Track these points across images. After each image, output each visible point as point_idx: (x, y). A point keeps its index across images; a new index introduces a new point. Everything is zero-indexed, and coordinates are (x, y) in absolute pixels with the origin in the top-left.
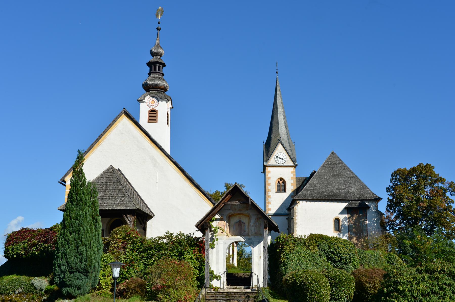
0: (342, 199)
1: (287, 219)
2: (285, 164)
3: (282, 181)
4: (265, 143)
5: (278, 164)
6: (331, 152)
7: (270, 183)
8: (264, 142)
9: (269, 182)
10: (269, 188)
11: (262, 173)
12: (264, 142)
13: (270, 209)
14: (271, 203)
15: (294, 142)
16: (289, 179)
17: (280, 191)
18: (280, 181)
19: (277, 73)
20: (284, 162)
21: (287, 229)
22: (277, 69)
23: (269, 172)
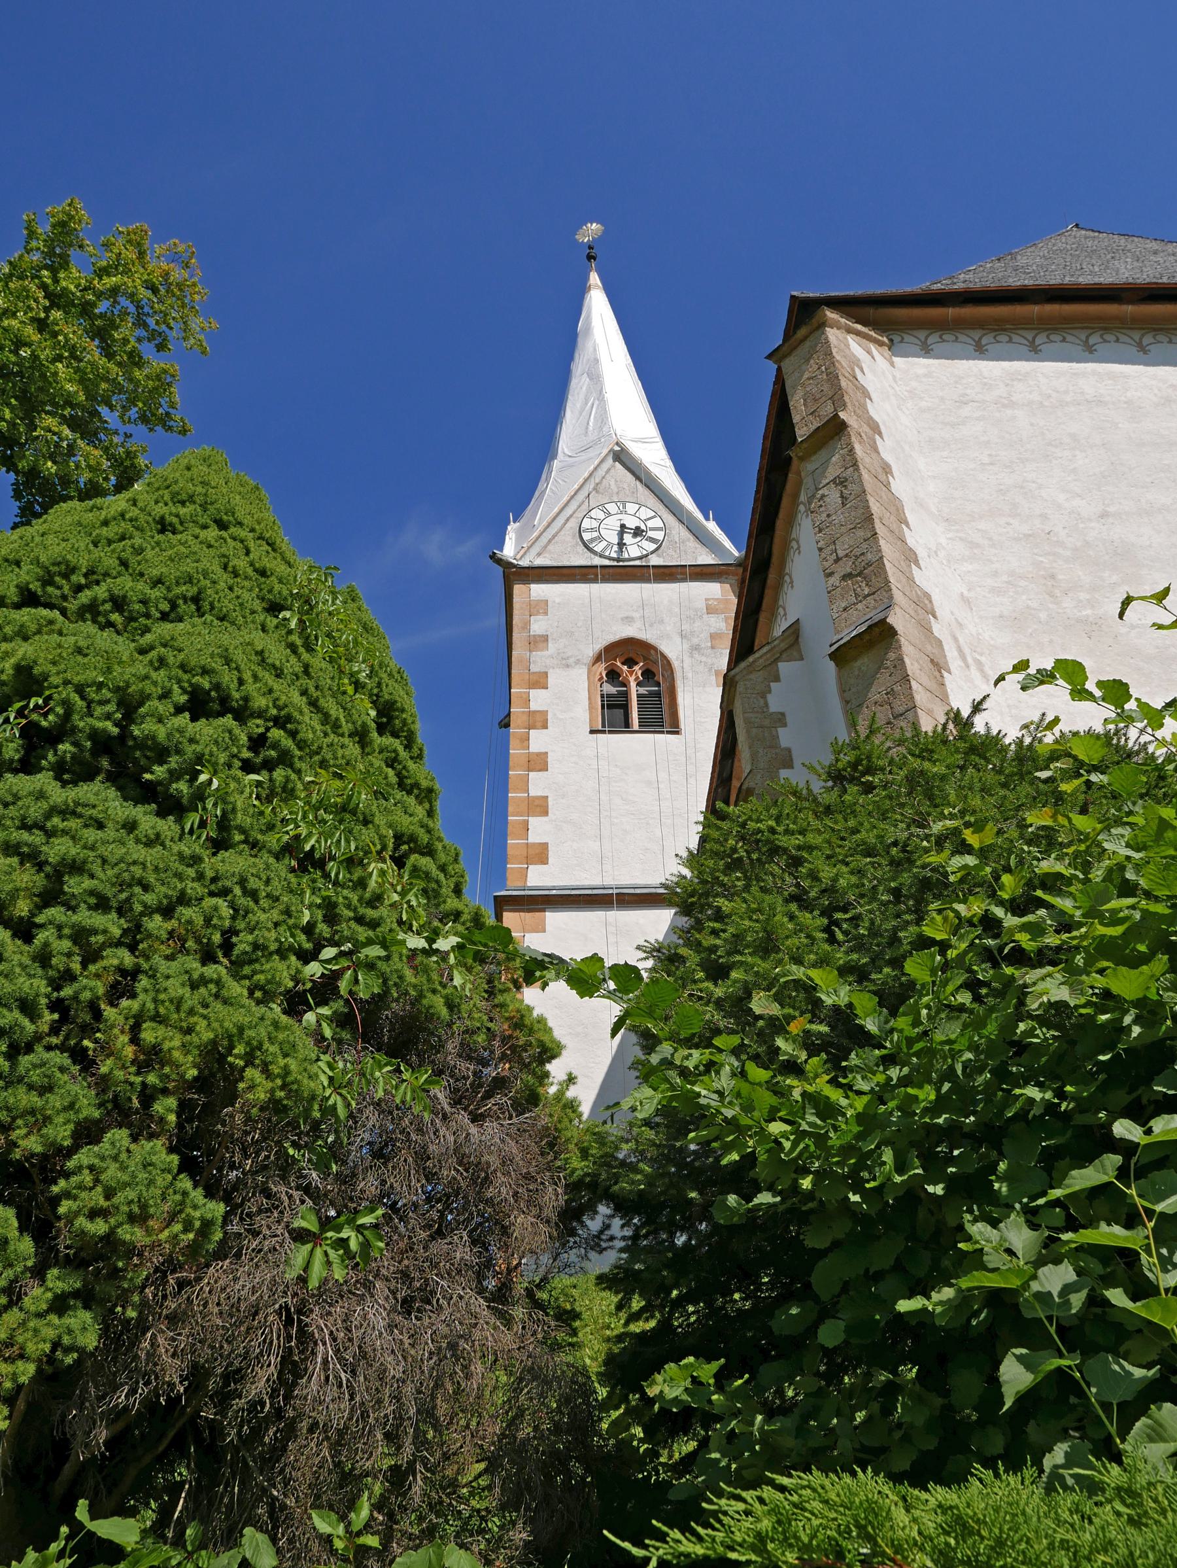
2: (655, 560)
5: (607, 562)
9: (534, 668)
13: (540, 855)
16: (696, 648)
17: (627, 723)
23: (541, 607)
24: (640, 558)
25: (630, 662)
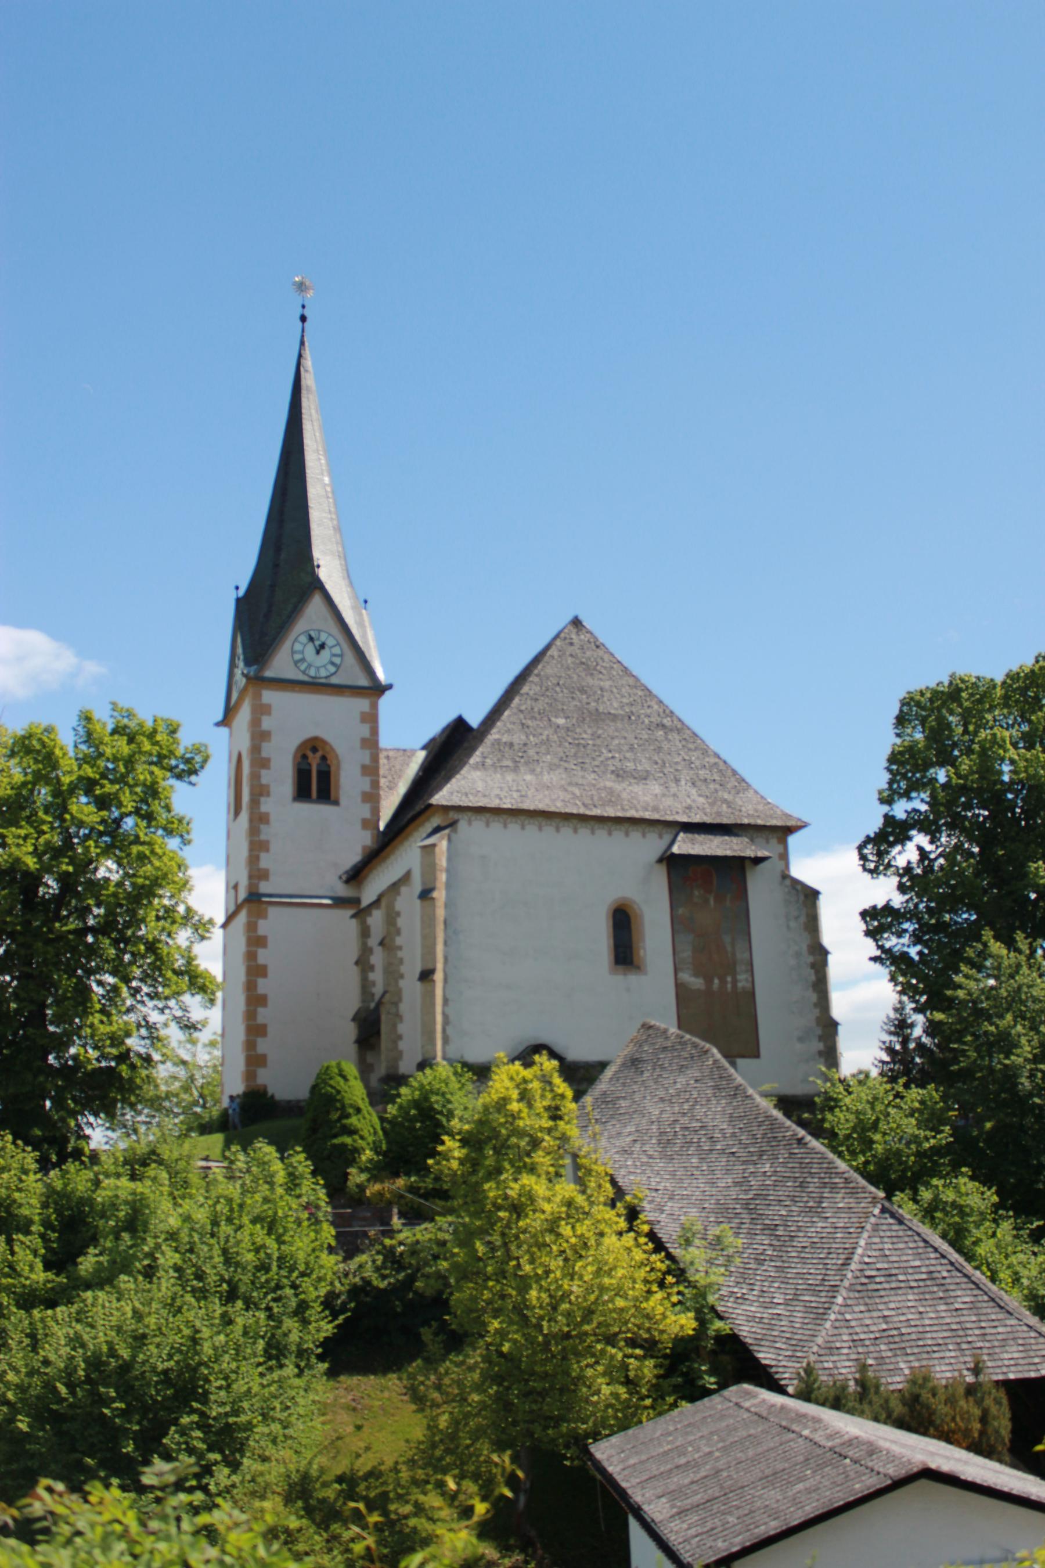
0: (647, 815)
1: (353, 916)
2: (334, 680)
3: (319, 755)
4: (241, 592)
5: (305, 678)
6: (569, 618)
7: (268, 760)
8: (237, 588)
10: (264, 781)
11: (218, 724)
12: (237, 588)
14: (273, 847)
15: (366, 602)
18: (310, 754)
19: (303, 319)
20: (332, 669)
21: (357, 963)
22: (303, 307)
24: (326, 677)
25: (314, 750)
